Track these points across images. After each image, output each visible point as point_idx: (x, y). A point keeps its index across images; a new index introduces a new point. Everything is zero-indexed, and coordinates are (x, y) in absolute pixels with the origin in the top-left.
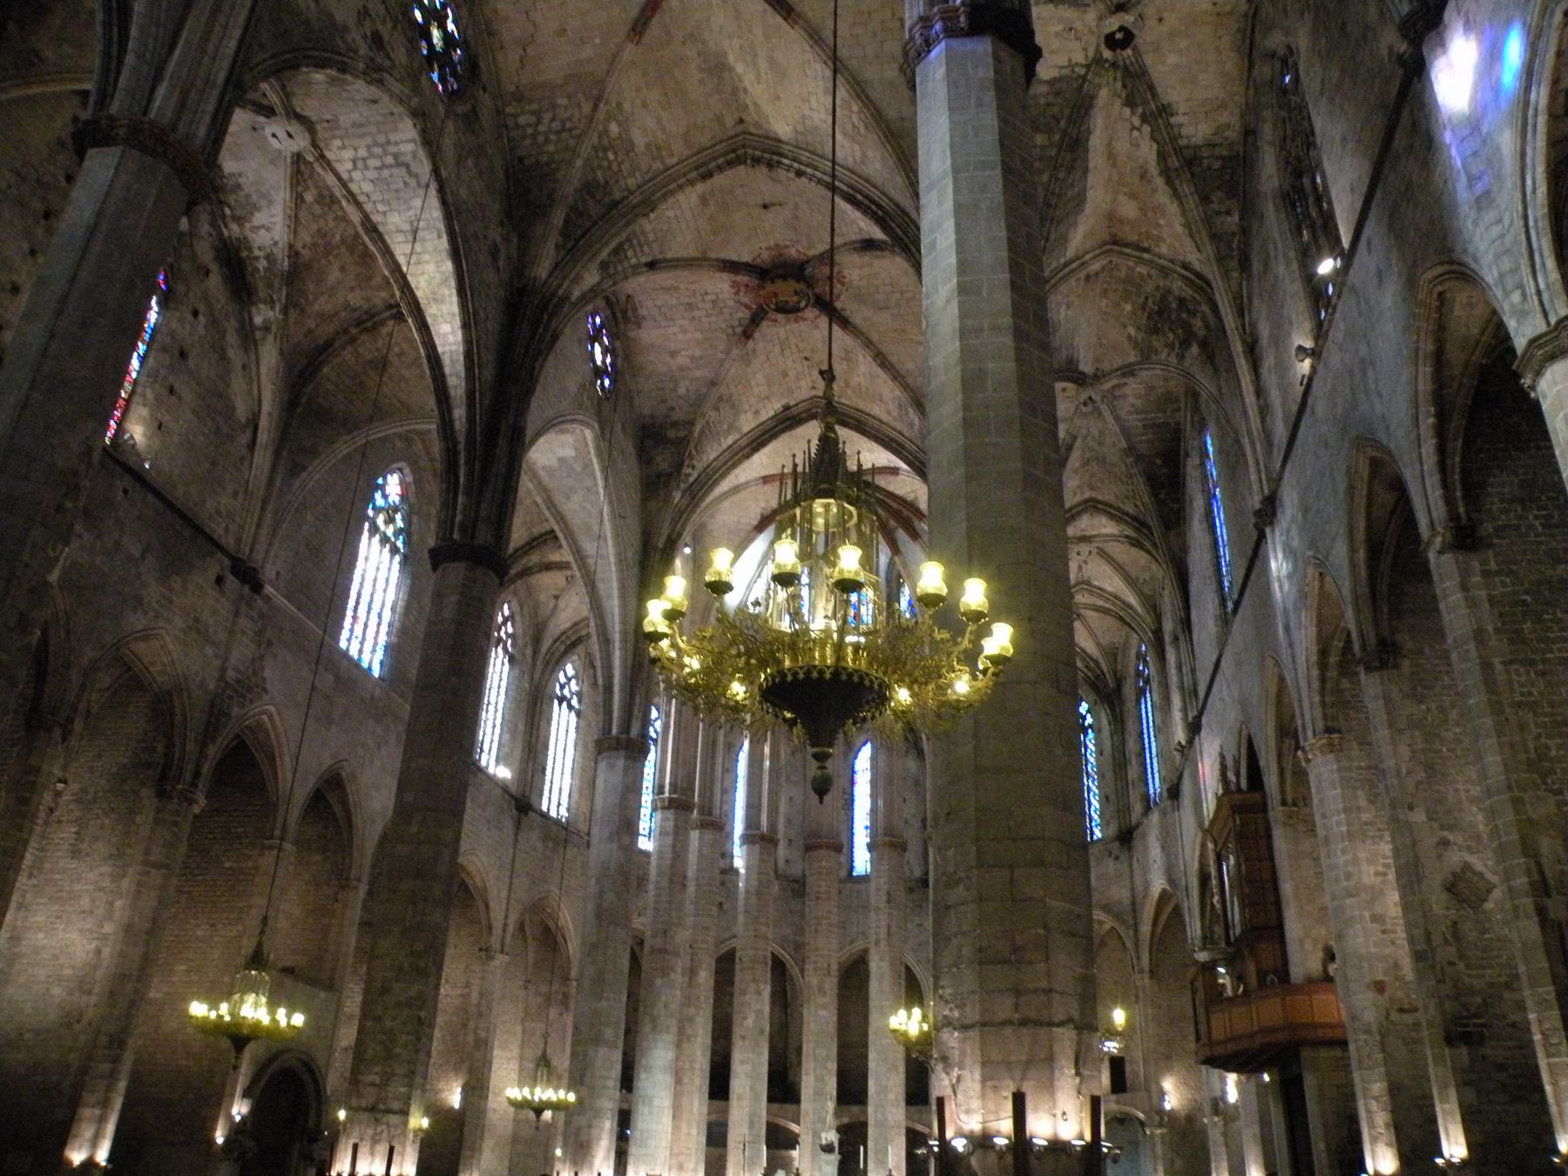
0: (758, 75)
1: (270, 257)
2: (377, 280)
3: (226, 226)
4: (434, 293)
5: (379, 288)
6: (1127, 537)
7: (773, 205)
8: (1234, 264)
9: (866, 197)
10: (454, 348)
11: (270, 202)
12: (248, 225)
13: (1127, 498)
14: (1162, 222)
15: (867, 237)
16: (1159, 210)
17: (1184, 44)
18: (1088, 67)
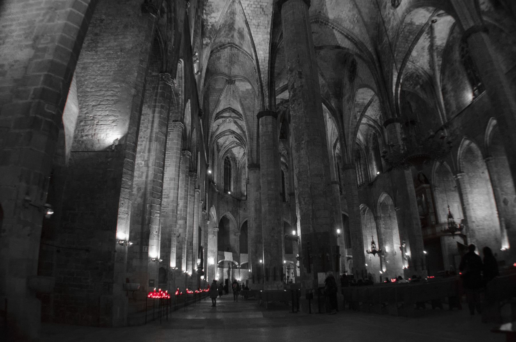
0: (331, 3)
1: (212, 26)
2: (230, 35)
3: (203, 16)
4: (259, 43)
5: (229, 38)
6: (367, 124)
7: (315, 33)
8: (439, 71)
9: (351, 37)
10: (262, 58)
11: (218, 11)
12: (209, 16)
13: (375, 115)
14: (421, 58)
15: (338, 45)
16: (423, 56)
17: (442, 25)
18: (425, 25)
